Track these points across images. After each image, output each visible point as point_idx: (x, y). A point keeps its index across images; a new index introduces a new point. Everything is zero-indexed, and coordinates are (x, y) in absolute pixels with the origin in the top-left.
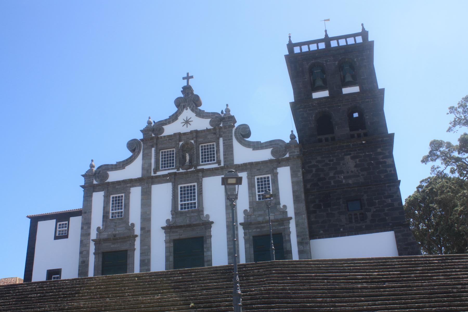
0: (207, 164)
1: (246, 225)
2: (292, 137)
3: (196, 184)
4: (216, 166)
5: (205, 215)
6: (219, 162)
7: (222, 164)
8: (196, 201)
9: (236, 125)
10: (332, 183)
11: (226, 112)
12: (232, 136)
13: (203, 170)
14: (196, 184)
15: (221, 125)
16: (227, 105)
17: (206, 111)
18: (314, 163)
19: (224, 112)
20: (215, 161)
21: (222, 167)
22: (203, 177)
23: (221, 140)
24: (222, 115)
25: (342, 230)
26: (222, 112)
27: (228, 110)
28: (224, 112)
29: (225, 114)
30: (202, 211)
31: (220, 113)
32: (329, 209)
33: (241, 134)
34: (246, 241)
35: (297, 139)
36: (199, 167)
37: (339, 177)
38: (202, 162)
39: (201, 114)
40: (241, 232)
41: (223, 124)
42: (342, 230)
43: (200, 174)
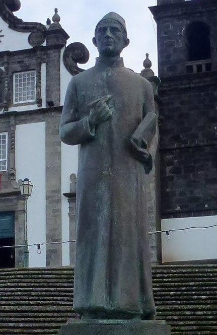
0: (22, 105)
1: (71, 196)
2: (147, 64)
3: (6, 134)
4: (35, 107)
5: (17, 181)
6: (39, 102)
7: (44, 106)
8: (6, 159)
9: (69, 42)
10: (200, 138)
11: (53, 21)
12: (59, 61)
13: (16, 114)
14: (6, 134)
15: (44, 44)
16: (56, 10)
17: (24, 20)
18: (177, 104)
19: (52, 22)
20: (34, 100)
21: (43, 109)
22: (16, 124)
23: (44, 66)
24: (48, 27)
25: (206, 206)
26: (48, 21)
27: (57, 19)
28: (52, 22)
29: (52, 26)
30: (13, 175)
31: (44, 23)
32: (192, 175)
33: (73, 59)
34: (72, 218)
35: (155, 69)
36: (11, 110)
37: (210, 127)
38: (17, 100)
39: (16, 25)
40: (65, 205)
41: (47, 42)
42: (206, 206)
43: (12, 118)
